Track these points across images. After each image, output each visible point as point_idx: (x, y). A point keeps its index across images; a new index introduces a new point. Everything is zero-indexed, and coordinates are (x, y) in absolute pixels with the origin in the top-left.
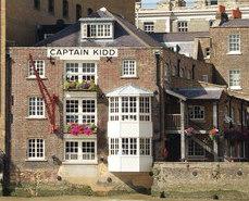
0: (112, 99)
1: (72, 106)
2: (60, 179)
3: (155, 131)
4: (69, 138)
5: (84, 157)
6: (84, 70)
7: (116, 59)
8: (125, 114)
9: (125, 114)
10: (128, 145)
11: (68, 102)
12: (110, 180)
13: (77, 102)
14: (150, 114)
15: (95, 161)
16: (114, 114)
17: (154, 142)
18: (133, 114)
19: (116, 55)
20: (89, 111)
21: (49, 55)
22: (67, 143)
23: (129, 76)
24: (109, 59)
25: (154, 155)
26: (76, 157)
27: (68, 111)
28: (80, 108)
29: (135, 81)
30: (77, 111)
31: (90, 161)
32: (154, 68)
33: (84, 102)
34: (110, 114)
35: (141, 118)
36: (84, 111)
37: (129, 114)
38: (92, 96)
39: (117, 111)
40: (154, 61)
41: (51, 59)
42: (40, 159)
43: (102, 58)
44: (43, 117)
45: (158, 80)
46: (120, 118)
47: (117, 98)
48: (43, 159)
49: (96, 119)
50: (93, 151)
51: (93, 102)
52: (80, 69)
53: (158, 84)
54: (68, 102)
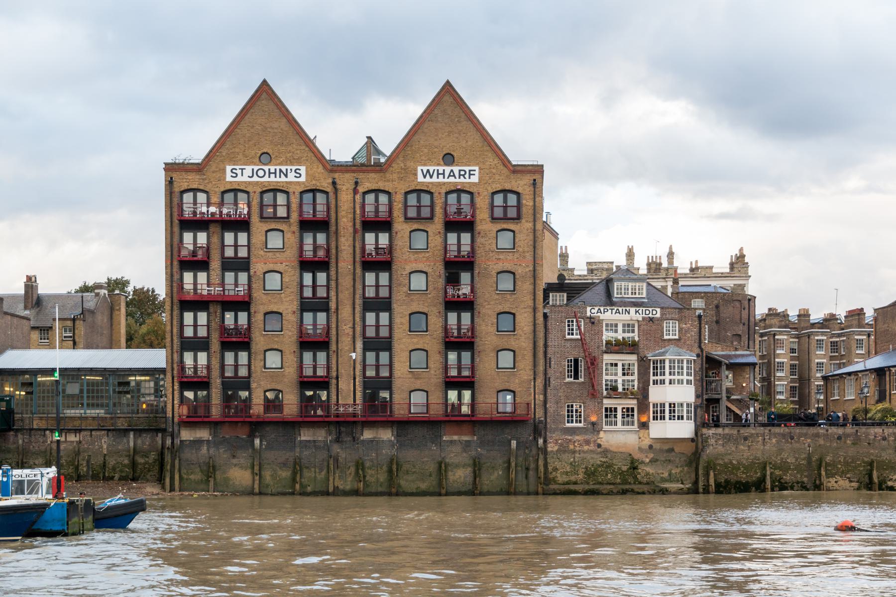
0: (655, 362)
2: (599, 446)
3: (697, 396)
4: (608, 403)
5: (623, 424)
6: (624, 331)
7: (658, 319)
9: (672, 377)
10: (674, 411)
12: (651, 447)
14: (692, 378)
15: (635, 427)
16: (659, 378)
17: (696, 407)
19: (658, 315)
21: (588, 314)
22: (606, 409)
23: (671, 337)
24: (651, 319)
25: (695, 421)
26: (616, 424)
31: (630, 428)
32: (696, 330)
34: (652, 378)
36: (624, 374)
37: (676, 377)
38: (633, 358)
41: (590, 318)
42: (579, 425)
43: (644, 319)
46: (667, 382)
48: (581, 425)
52: (620, 328)
53: (700, 347)
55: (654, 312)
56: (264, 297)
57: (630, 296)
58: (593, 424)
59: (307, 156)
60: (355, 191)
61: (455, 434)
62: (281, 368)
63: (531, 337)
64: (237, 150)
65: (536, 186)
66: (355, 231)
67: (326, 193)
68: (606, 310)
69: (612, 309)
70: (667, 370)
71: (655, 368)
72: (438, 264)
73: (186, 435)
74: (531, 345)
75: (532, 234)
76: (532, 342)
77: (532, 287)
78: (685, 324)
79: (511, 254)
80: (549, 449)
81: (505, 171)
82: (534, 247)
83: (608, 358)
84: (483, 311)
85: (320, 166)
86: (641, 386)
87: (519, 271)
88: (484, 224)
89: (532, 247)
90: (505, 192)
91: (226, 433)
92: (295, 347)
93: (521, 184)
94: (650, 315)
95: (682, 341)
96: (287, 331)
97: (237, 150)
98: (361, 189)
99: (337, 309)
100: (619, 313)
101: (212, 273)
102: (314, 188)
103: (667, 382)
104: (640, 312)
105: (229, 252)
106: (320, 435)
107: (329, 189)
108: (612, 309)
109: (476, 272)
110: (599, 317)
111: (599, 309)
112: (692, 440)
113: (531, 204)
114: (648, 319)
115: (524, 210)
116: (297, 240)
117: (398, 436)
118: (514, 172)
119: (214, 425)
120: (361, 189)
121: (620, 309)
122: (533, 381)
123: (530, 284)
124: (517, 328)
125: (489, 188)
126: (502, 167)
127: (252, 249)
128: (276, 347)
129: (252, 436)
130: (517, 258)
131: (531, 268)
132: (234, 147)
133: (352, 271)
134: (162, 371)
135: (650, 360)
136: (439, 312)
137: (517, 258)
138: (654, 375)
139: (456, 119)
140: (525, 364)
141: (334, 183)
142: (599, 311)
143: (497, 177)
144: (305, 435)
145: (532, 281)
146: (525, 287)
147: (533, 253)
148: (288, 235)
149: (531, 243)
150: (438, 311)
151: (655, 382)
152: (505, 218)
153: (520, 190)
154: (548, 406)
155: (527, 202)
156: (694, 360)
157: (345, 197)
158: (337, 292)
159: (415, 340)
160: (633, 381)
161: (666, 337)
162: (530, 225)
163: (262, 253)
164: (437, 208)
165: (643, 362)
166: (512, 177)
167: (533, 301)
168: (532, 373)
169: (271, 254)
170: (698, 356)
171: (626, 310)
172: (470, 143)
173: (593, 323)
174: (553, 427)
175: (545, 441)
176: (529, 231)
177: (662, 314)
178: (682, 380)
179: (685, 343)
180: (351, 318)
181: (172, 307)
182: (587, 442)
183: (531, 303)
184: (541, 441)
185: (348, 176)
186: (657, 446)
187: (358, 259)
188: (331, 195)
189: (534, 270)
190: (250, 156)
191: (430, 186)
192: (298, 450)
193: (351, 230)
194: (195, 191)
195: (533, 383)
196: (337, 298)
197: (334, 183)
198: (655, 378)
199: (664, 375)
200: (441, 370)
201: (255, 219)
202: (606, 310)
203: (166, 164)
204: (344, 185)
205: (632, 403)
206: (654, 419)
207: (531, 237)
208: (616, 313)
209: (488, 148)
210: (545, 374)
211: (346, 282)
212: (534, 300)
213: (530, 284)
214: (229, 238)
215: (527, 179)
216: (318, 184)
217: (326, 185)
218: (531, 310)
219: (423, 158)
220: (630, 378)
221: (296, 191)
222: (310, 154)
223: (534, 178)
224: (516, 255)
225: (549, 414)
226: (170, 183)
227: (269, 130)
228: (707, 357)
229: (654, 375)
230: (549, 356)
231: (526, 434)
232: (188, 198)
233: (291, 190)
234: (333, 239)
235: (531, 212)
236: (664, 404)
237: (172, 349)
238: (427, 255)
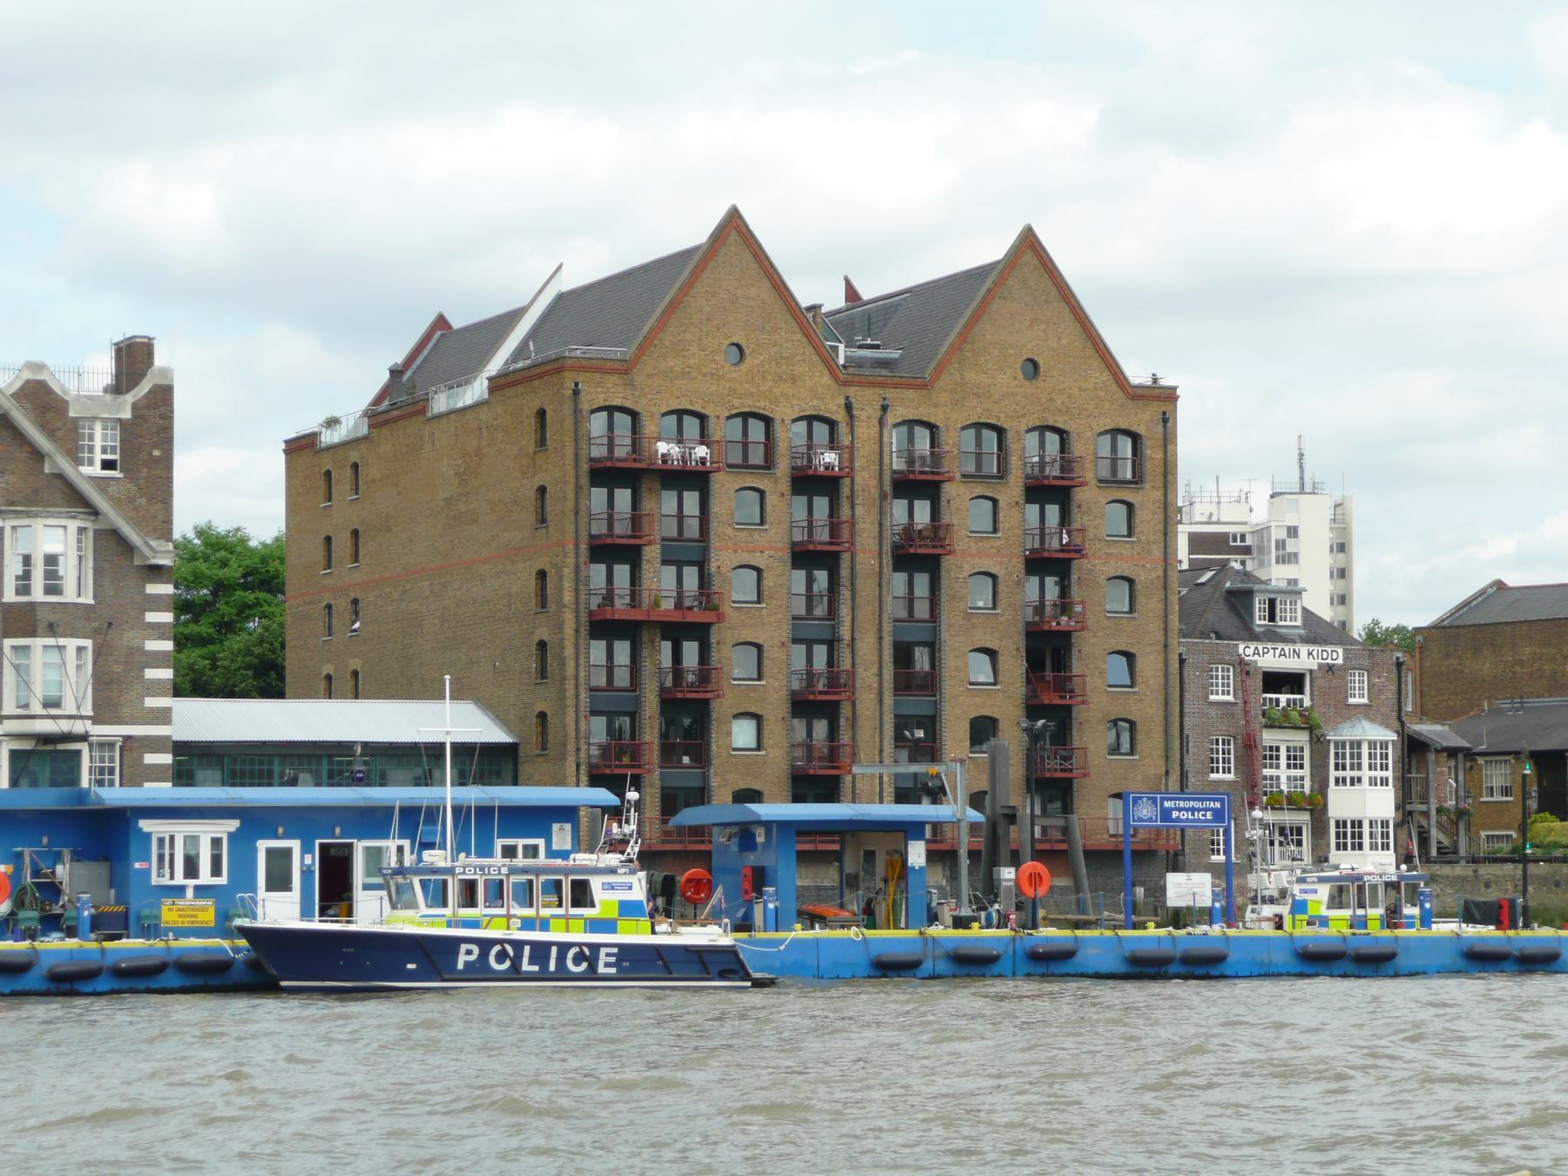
0: (1340, 745)
7: (1340, 668)
13: (1278, 749)
16: (1348, 774)
17: (1396, 826)
19: (1340, 661)
20: (1295, 766)
24: (1330, 668)
25: (1395, 851)
28: (1283, 761)
29: (1366, 711)
30: (1278, 767)
32: (1394, 688)
33: (1288, 749)
34: (1333, 774)
36: (1289, 766)
38: (1301, 738)
40: (1394, 675)
43: (1320, 665)
44: (1231, 777)
47: (1359, 744)
50: (1299, 843)
51: (1302, 749)
55: (1335, 656)
56: (734, 615)
59: (804, 353)
60: (881, 422)
62: (759, 748)
63: (1161, 698)
64: (688, 336)
65: (1167, 420)
66: (883, 496)
67: (832, 424)
68: (1266, 650)
69: (1275, 649)
70: (1365, 761)
72: (1015, 561)
74: (1161, 712)
75: (1162, 510)
76: (1161, 706)
77: (1161, 606)
78: (1379, 678)
79: (1128, 546)
81: (1120, 394)
82: (1166, 534)
83: (1269, 737)
84: (1086, 649)
85: (826, 372)
86: (1316, 787)
87: (1141, 578)
89: (1161, 535)
93: (1142, 420)
94: (1329, 661)
95: (1375, 708)
96: (771, 680)
97: (688, 336)
98: (891, 419)
99: (853, 639)
100: (1285, 655)
101: (645, 566)
102: (816, 413)
103: (1365, 781)
104: (1315, 653)
107: (840, 416)
108: (1275, 649)
110: (1256, 662)
111: (1256, 648)
113: (1159, 455)
114: (1326, 668)
121: (1286, 649)
122: (1164, 778)
123: (1158, 601)
124: (1139, 679)
125: (1095, 426)
126: (1115, 387)
128: (752, 709)
130: (1138, 554)
131: (1160, 573)
132: (684, 331)
133: (877, 569)
135: (1329, 741)
136: (1018, 649)
137: (1138, 554)
138: (1337, 768)
139: (1043, 297)
141: (848, 407)
143: (1107, 405)
145: (1162, 596)
146: (1150, 604)
147: (1162, 545)
148: (771, 500)
149: (1160, 527)
150: (1015, 647)
153: (1141, 430)
155: (1152, 453)
156: (1393, 741)
157: (866, 430)
158: (853, 609)
159: (978, 700)
160: (1302, 778)
161: (1351, 701)
162: (1158, 493)
163: (730, 531)
164: (1014, 458)
166: (1130, 406)
167: (1162, 633)
168: (1162, 763)
169: (744, 534)
171: (1294, 651)
172: (1064, 342)
173: (1248, 673)
174: (1193, 861)
176: (1157, 504)
177: (1345, 659)
178: (1344, 780)
179: (1378, 710)
180: (876, 658)
181: (577, 631)
183: (1159, 636)
188: (843, 429)
189: (1165, 577)
190: (711, 349)
191: (1003, 419)
193: (875, 493)
195: (1163, 781)
196: (853, 620)
197: (848, 407)
198: (1340, 774)
199: (1359, 768)
200: (1020, 756)
202: (1266, 650)
204: (863, 409)
205: (1303, 818)
206: (1338, 848)
207: (1160, 516)
208: (1280, 655)
209: (1092, 352)
210: (1182, 765)
211: (867, 588)
213: (1158, 601)
214: (669, 501)
215: (1155, 409)
216: (823, 407)
217: (835, 408)
218: (1160, 648)
219: (990, 365)
221: (786, 418)
222: (810, 350)
223: (1164, 409)
225: (1187, 838)
227: (741, 301)
229: (1337, 768)
230: (1186, 732)
233: (777, 416)
234: (845, 512)
235: (1160, 470)
236: (1360, 824)
237: (577, 712)
238: (998, 543)
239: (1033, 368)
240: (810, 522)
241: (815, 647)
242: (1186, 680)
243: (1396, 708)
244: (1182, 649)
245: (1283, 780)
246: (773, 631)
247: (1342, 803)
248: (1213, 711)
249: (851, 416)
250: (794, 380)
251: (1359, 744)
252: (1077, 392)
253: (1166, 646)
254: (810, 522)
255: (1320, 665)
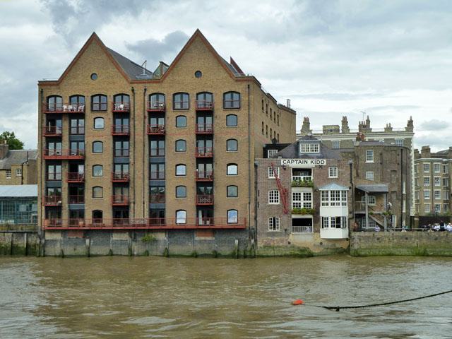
0: (323, 192)
1: (297, 196)
2: (289, 243)
3: (350, 213)
7: (325, 166)
8: (333, 201)
9: (333, 201)
11: (294, 194)
12: (321, 243)
13: (300, 194)
14: (346, 201)
16: (325, 202)
17: (349, 219)
18: (338, 201)
19: (325, 164)
21: (282, 164)
24: (321, 166)
27: (294, 200)
28: (302, 198)
29: (336, 180)
30: (300, 200)
32: (349, 172)
33: (304, 194)
34: (321, 202)
35: (343, 204)
36: (304, 200)
37: (335, 201)
38: (310, 190)
39: (327, 199)
40: (349, 168)
41: (283, 166)
43: (316, 166)
44: (278, 203)
45: (351, 179)
46: (330, 204)
47: (327, 192)
49: (312, 205)
51: (310, 194)
53: (351, 182)
54: (294, 194)
57: (310, 152)
58: (286, 230)
61: (203, 236)
66: (145, 117)
71: (323, 196)
73: (48, 236)
80: (258, 245)
81: (231, 80)
83: (294, 190)
87: (240, 139)
88: (220, 113)
90: (232, 92)
91: (73, 237)
92: (110, 185)
98: (148, 93)
103: (330, 204)
105: (74, 131)
106: (125, 237)
107: (130, 93)
109: (214, 140)
112: (347, 239)
113: (247, 99)
115: (242, 103)
116: (111, 123)
117: (169, 237)
118: (237, 81)
119: (64, 231)
120: (148, 93)
127: (86, 129)
129: (84, 237)
131: (247, 137)
134: (35, 198)
140: (244, 194)
141: (133, 90)
142: (289, 162)
144: (115, 237)
151: (323, 204)
152: (232, 108)
154: (258, 219)
157: (139, 97)
158: (134, 153)
165: (316, 191)
170: (350, 188)
175: (256, 241)
177: (327, 163)
182: (282, 241)
184: (253, 241)
185: (141, 85)
186: (325, 243)
187: (146, 132)
189: (249, 138)
192: (111, 245)
194: (55, 96)
197: (133, 90)
198: (323, 202)
201: (88, 112)
203: (39, 82)
211: (139, 147)
212: (249, 156)
214: (74, 122)
220: (309, 201)
224: (238, 129)
226: (41, 92)
228: (356, 189)
231: (245, 237)
232: (51, 101)
234: (132, 122)
239: (198, 74)
240: (122, 127)
241: (124, 165)
242: (258, 172)
243: (349, 179)
244: (256, 162)
245: (302, 204)
246: (106, 160)
247: (327, 212)
248: (270, 182)
249: (134, 93)
250: (114, 83)
251: (327, 192)
252: (215, 80)
253: (249, 161)
254: (122, 127)
255: (316, 166)
